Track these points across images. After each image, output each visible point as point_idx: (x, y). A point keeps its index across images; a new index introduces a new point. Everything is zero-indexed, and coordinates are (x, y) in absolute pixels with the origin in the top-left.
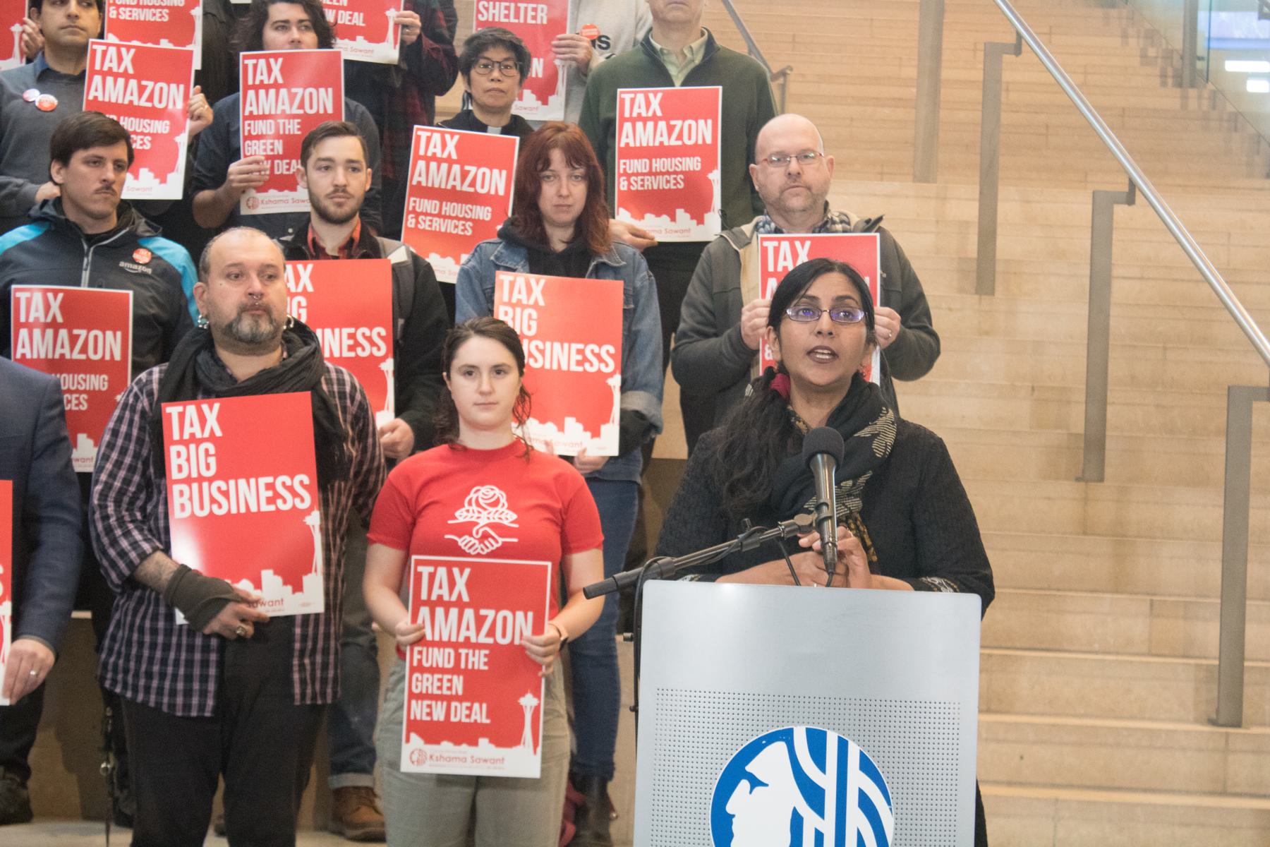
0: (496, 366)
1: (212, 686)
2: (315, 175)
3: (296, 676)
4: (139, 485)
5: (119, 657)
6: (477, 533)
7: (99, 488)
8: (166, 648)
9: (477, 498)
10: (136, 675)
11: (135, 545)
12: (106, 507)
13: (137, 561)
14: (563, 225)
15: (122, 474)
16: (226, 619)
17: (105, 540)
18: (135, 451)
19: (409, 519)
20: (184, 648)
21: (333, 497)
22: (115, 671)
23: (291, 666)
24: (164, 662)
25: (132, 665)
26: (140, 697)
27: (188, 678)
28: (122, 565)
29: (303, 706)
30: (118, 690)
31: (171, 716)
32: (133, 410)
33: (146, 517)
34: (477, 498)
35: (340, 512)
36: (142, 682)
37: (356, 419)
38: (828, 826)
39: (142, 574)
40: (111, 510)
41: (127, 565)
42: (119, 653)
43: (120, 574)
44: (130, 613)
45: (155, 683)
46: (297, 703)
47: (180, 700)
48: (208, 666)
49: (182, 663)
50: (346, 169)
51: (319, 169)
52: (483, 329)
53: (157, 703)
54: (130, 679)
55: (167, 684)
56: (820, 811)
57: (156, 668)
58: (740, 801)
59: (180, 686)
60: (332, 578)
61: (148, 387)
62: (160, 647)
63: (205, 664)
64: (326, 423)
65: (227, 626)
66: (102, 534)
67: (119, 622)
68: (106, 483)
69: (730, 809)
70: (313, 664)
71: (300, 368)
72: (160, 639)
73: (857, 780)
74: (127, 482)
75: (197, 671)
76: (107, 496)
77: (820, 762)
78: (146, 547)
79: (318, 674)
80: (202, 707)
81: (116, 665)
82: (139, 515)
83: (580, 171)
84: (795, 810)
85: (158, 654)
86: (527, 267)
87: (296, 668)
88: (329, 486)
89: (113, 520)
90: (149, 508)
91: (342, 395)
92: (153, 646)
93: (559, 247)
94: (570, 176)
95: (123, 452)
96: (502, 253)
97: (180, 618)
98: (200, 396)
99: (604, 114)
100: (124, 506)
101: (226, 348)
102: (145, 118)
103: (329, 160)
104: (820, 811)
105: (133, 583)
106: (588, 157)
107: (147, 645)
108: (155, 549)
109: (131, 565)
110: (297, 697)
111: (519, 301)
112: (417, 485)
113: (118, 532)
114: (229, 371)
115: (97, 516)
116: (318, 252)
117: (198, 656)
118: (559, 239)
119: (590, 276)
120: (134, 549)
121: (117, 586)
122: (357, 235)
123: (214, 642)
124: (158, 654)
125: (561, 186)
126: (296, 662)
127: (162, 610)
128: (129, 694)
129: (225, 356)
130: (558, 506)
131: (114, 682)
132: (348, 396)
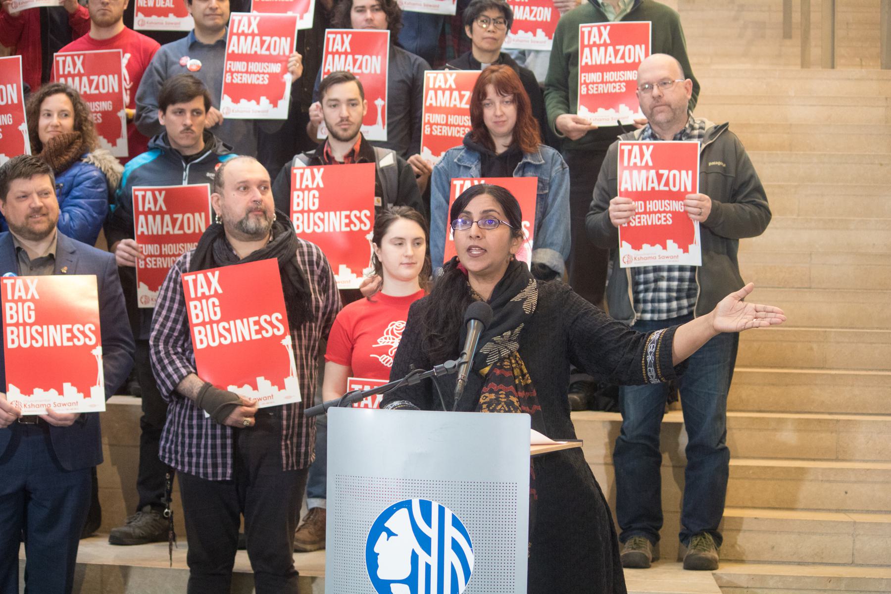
1: (229, 461)
2: (328, 110)
3: (283, 452)
4: (180, 331)
5: (172, 444)
6: (391, 353)
7: (154, 334)
8: (199, 437)
9: (392, 330)
10: (183, 456)
11: (177, 370)
12: (158, 346)
13: (177, 381)
14: (505, 135)
15: (169, 324)
16: (234, 417)
17: (159, 367)
18: (178, 310)
19: (351, 347)
20: (209, 437)
21: (305, 333)
22: (170, 453)
23: (281, 445)
24: (198, 446)
25: (179, 448)
26: (186, 469)
27: (214, 456)
28: (168, 383)
29: (287, 470)
30: (173, 465)
31: (205, 481)
32: (175, 282)
33: (184, 351)
34: (392, 330)
35: (312, 342)
36: (186, 459)
37: (321, 278)
38: (433, 561)
39: (182, 388)
40: (161, 347)
41: (172, 383)
42: (172, 441)
43: (168, 389)
44: (177, 414)
45: (194, 460)
46: (284, 470)
47: (210, 470)
48: (226, 448)
49: (209, 446)
50: (348, 105)
53: (196, 472)
54: (179, 459)
55: (201, 460)
56: (429, 553)
57: (194, 450)
58: (382, 545)
59: (209, 461)
60: (306, 387)
61: (184, 267)
62: (195, 436)
63: (224, 446)
64: (298, 285)
65: (237, 421)
66: (156, 363)
67: (171, 420)
68: (159, 330)
69: (376, 549)
70: (292, 443)
71: (281, 247)
72: (195, 431)
73: (451, 532)
74: (172, 329)
75: (219, 451)
76: (159, 339)
78: (184, 371)
79: (295, 450)
80: (224, 474)
81: (170, 448)
82: (180, 350)
83: (509, 98)
84: (413, 550)
85: (195, 441)
87: (283, 447)
88: (302, 327)
89: (162, 354)
90: (186, 345)
91: (311, 263)
92: (191, 436)
93: (500, 149)
94: (502, 102)
95: (170, 310)
97: (207, 415)
100: (170, 344)
101: (234, 237)
104: (429, 552)
105: (177, 395)
106: (514, 88)
107: (187, 436)
108: (189, 373)
109: (173, 383)
110: (284, 466)
112: (353, 324)
113: (166, 361)
114: (235, 252)
115: (152, 351)
117: (219, 441)
120: (176, 373)
121: (166, 397)
123: (229, 432)
124: (195, 441)
125: (496, 109)
126: (283, 443)
127: (195, 413)
128: (179, 468)
129: (235, 243)
131: (170, 460)
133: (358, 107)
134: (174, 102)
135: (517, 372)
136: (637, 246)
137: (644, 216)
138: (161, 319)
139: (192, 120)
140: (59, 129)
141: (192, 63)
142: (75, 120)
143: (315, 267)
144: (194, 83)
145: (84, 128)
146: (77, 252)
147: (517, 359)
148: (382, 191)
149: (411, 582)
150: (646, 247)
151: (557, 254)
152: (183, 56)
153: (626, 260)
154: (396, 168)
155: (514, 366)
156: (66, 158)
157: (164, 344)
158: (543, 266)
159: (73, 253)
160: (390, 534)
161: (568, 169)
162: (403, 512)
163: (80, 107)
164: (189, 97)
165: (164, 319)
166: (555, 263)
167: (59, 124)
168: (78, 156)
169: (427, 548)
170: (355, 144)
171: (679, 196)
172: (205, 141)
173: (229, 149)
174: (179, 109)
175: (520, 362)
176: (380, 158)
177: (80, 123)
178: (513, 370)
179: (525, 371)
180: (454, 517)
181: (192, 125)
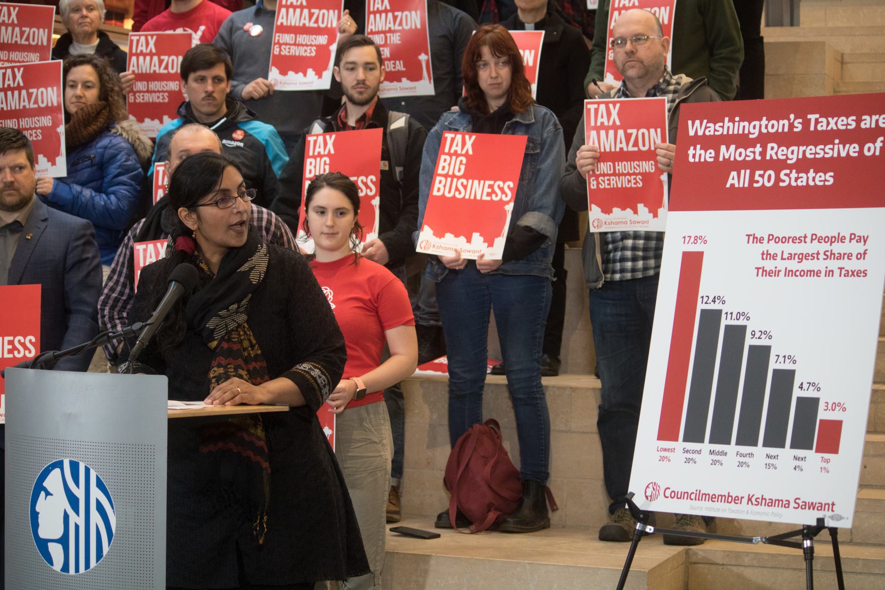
0: (338, 209)
7: (102, 298)
40: (106, 312)
51: (347, 69)
52: (334, 182)
68: (107, 294)
74: (121, 293)
76: (107, 303)
86: (470, 127)
89: (106, 319)
96: (455, 119)
98: (163, 236)
99: (606, 9)
102: (312, 35)
103: (353, 63)
111: (456, 151)
115: (99, 316)
116: (344, 127)
118: (494, 105)
119: (505, 133)
122: (370, 112)
130: (367, 297)
132: (264, 228)
133: (374, 71)
134: (195, 70)
135: (246, 344)
136: (607, 210)
137: (614, 178)
138: (111, 284)
139: (214, 87)
140: (83, 100)
141: (256, 30)
142: (101, 90)
143: (264, 233)
144: (214, 50)
145: (110, 99)
146: (50, 220)
147: (246, 329)
148: (389, 154)
150: (616, 211)
151: (546, 217)
152: (248, 22)
153: (595, 224)
154: (407, 131)
155: (242, 338)
156: (93, 128)
157: (110, 309)
158: (528, 229)
159: (45, 220)
161: (562, 130)
163: (106, 77)
164: (210, 65)
165: (115, 283)
166: (542, 226)
167: (82, 95)
168: (106, 125)
169: (77, 511)
170: (368, 109)
171: (650, 155)
172: (228, 107)
173: (253, 116)
174: (200, 76)
175: (248, 333)
176: (392, 120)
177: (105, 95)
178: (242, 342)
179: (254, 342)
181: (213, 92)
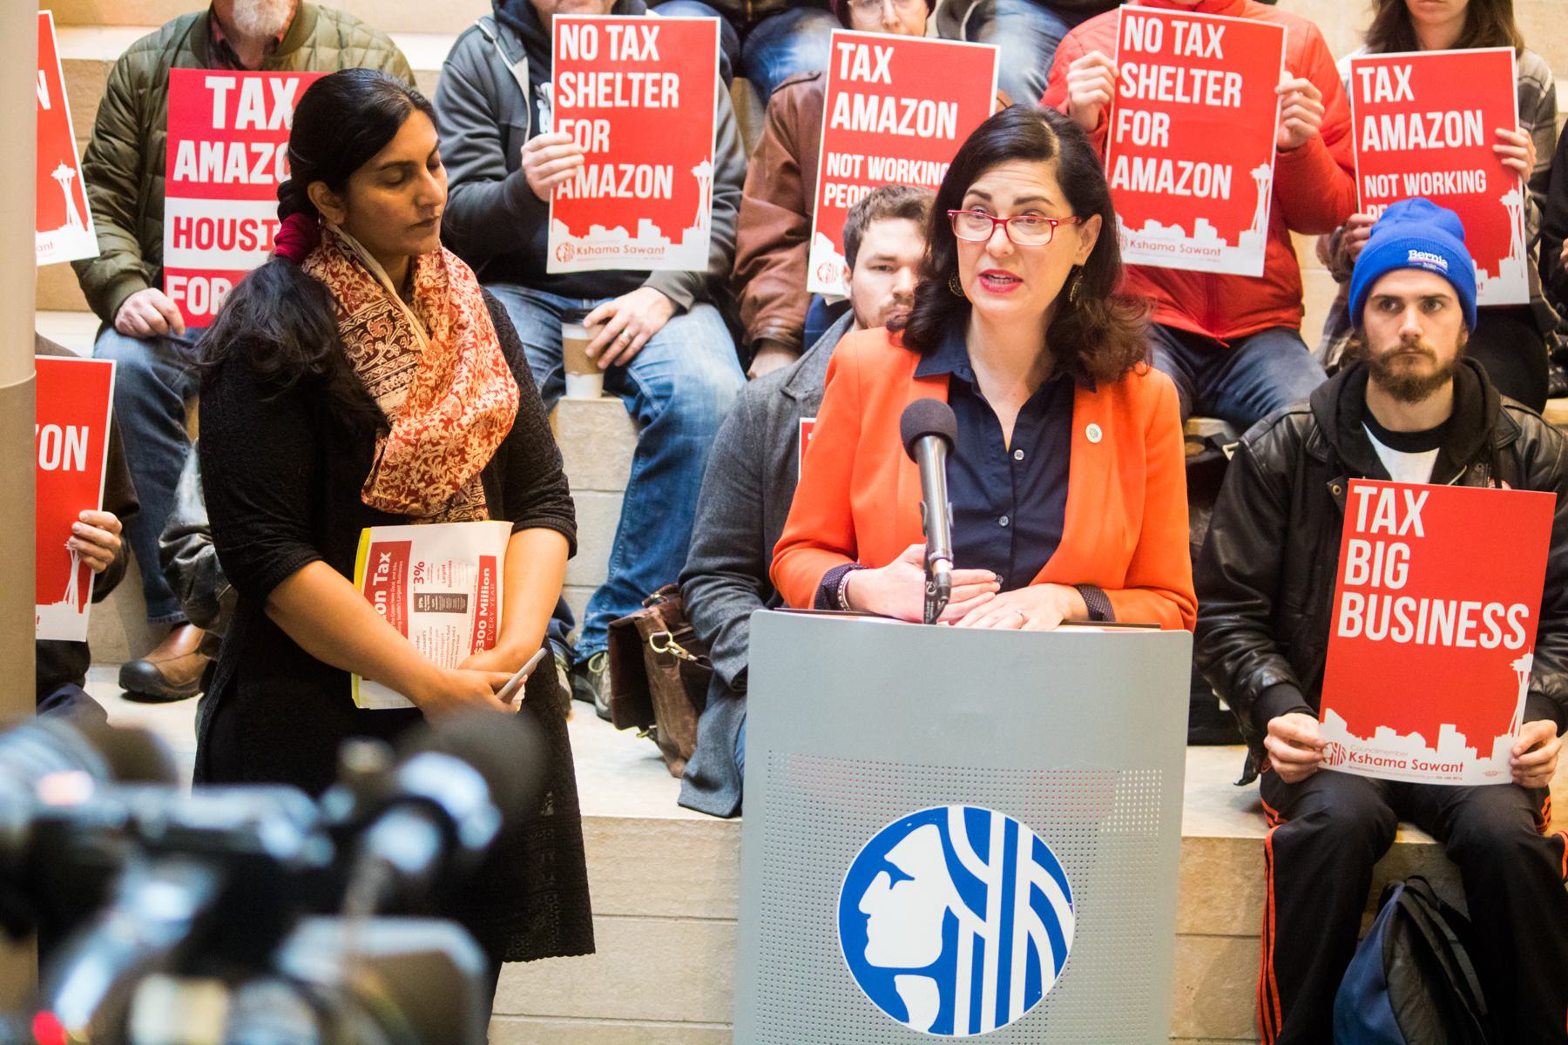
38: (990, 930)
56: (983, 916)
58: (877, 897)
69: (864, 906)
73: (1029, 872)
77: (980, 845)
84: (948, 909)
104: (981, 912)
149: (943, 972)
160: (897, 875)
162: (930, 832)
180: (1037, 844)
